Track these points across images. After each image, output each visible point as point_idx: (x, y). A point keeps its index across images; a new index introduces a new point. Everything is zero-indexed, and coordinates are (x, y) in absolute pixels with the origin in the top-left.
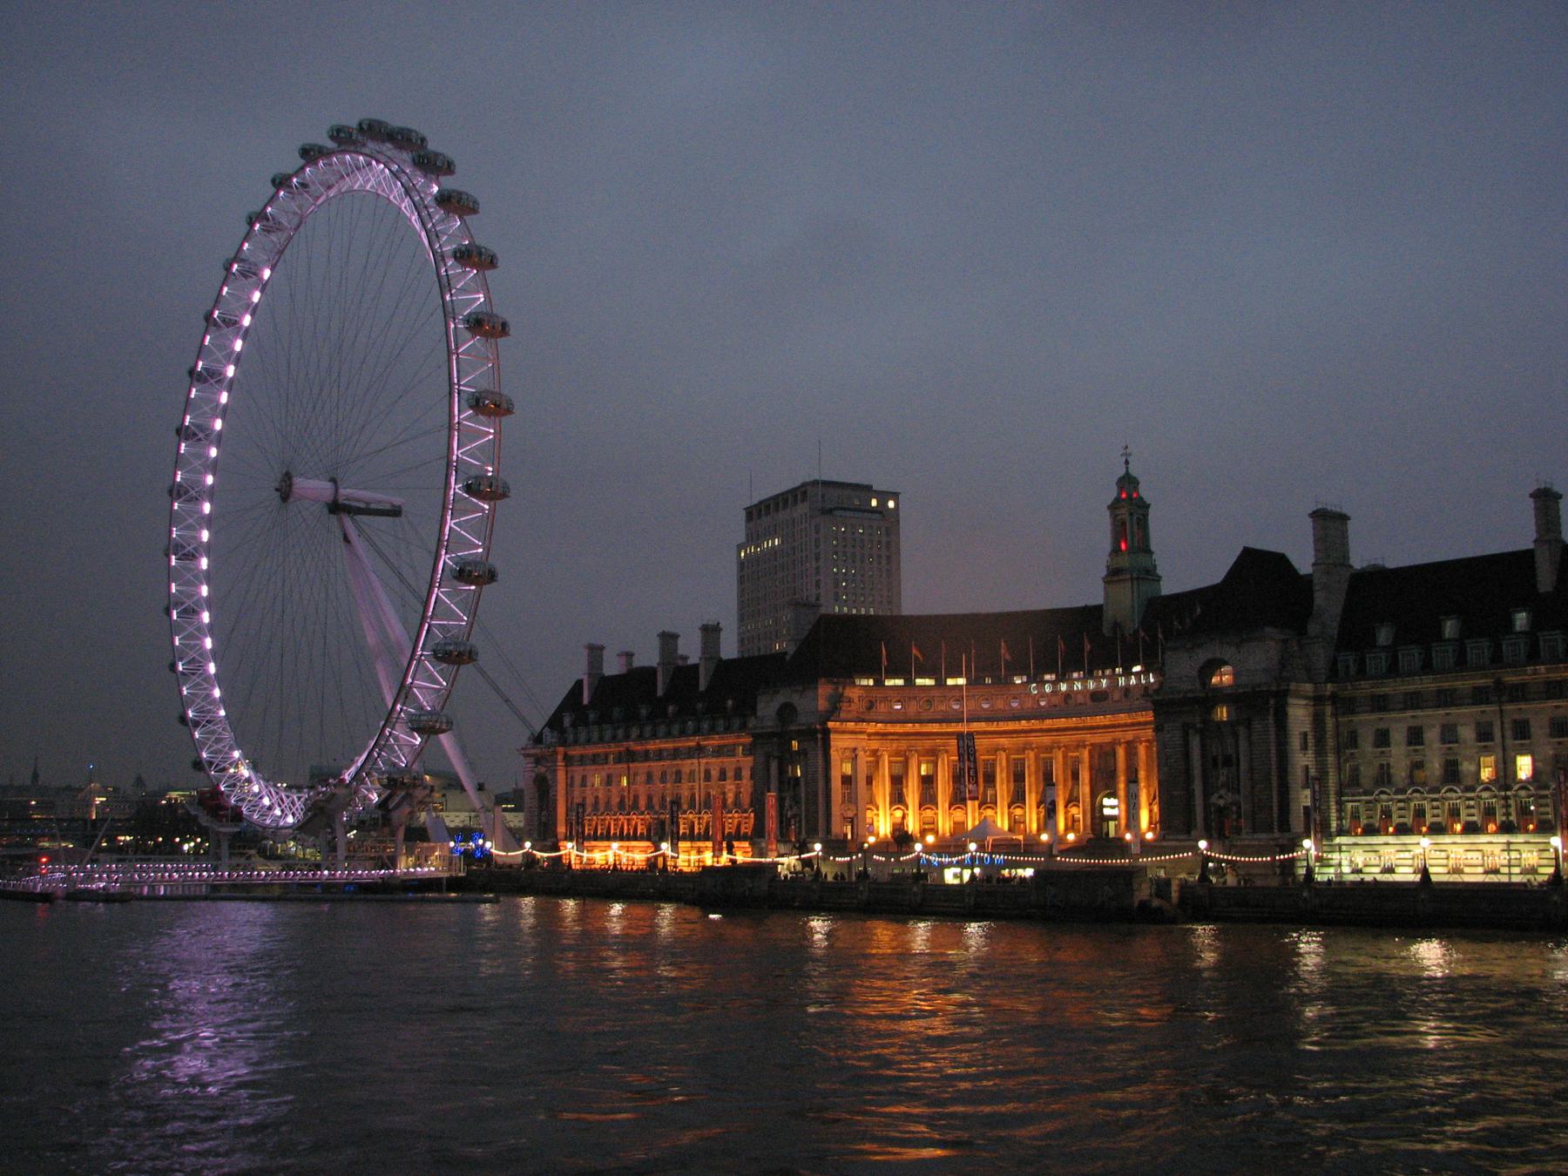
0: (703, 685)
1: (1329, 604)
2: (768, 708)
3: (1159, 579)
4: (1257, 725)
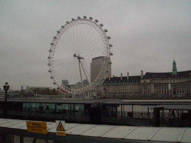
0: (128, 79)
2: (142, 81)
3: (177, 70)
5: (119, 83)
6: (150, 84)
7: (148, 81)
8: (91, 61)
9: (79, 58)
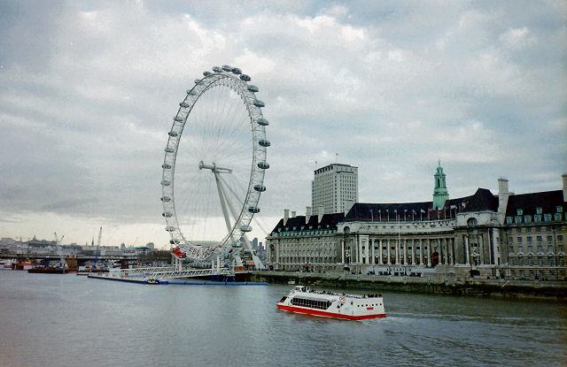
0: (319, 221)
1: (503, 204)
2: (341, 228)
4: (484, 235)
5: (300, 233)
6: (356, 235)
7: (354, 227)
8: (312, 177)
9: (213, 170)
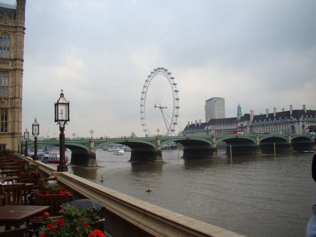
1: (252, 118)
2: (206, 128)
7: (210, 128)
8: (205, 104)
9: (160, 108)
